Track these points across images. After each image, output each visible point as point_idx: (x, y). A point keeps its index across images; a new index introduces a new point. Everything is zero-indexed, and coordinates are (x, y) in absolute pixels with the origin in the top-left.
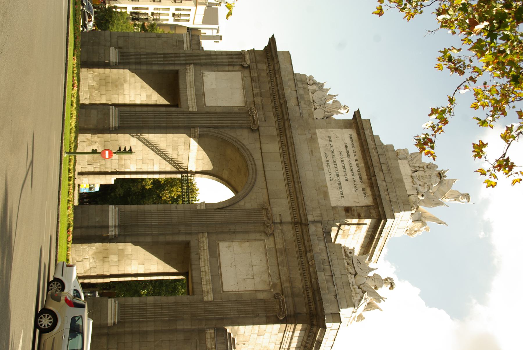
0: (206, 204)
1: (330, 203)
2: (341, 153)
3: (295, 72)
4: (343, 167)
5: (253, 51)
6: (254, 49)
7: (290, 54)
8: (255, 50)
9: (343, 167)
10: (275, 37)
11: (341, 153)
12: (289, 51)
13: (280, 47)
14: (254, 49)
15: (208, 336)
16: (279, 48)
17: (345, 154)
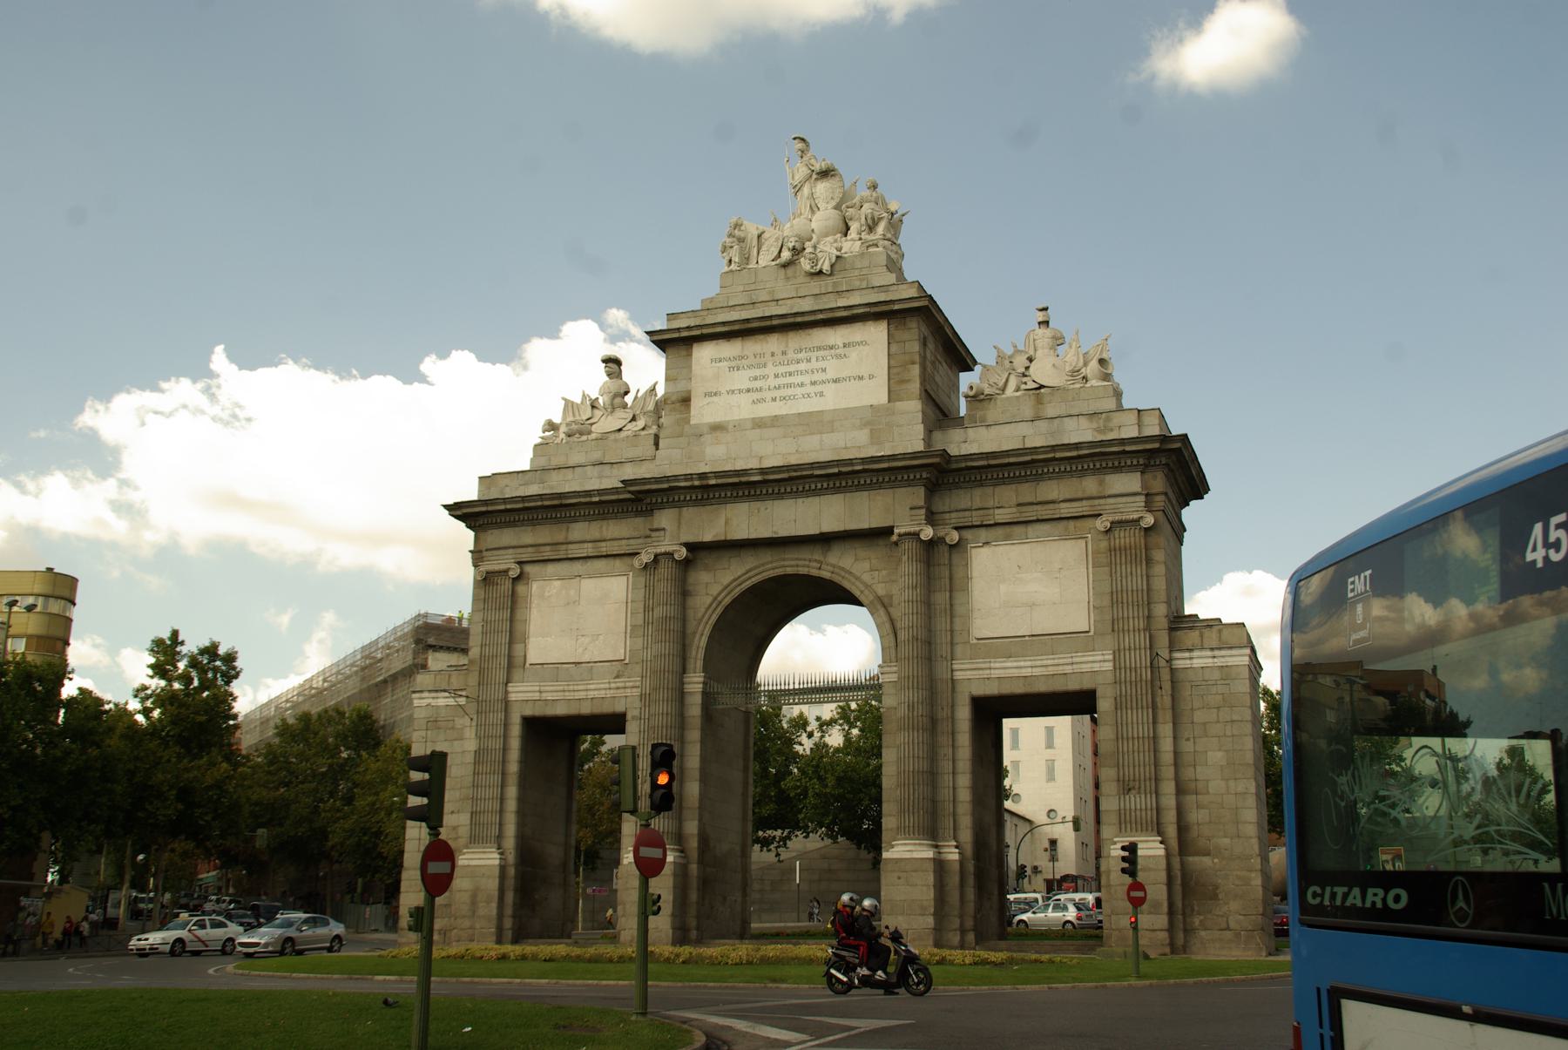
0: (884, 661)
1: (883, 405)
2: (756, 379)
3: (527, 467)
4: (790, 375)
5: (478, 555)
6: (470, 551)
7: (489, 474)
8: (472, 548)
9: (790, 375)
10: (451, 502)
11: (756, 379)
12: (480, 478)
13: (470, 493)
14: (470, 551)
15: (1187, 663)
16: (472, 494)
17: (757, 372)
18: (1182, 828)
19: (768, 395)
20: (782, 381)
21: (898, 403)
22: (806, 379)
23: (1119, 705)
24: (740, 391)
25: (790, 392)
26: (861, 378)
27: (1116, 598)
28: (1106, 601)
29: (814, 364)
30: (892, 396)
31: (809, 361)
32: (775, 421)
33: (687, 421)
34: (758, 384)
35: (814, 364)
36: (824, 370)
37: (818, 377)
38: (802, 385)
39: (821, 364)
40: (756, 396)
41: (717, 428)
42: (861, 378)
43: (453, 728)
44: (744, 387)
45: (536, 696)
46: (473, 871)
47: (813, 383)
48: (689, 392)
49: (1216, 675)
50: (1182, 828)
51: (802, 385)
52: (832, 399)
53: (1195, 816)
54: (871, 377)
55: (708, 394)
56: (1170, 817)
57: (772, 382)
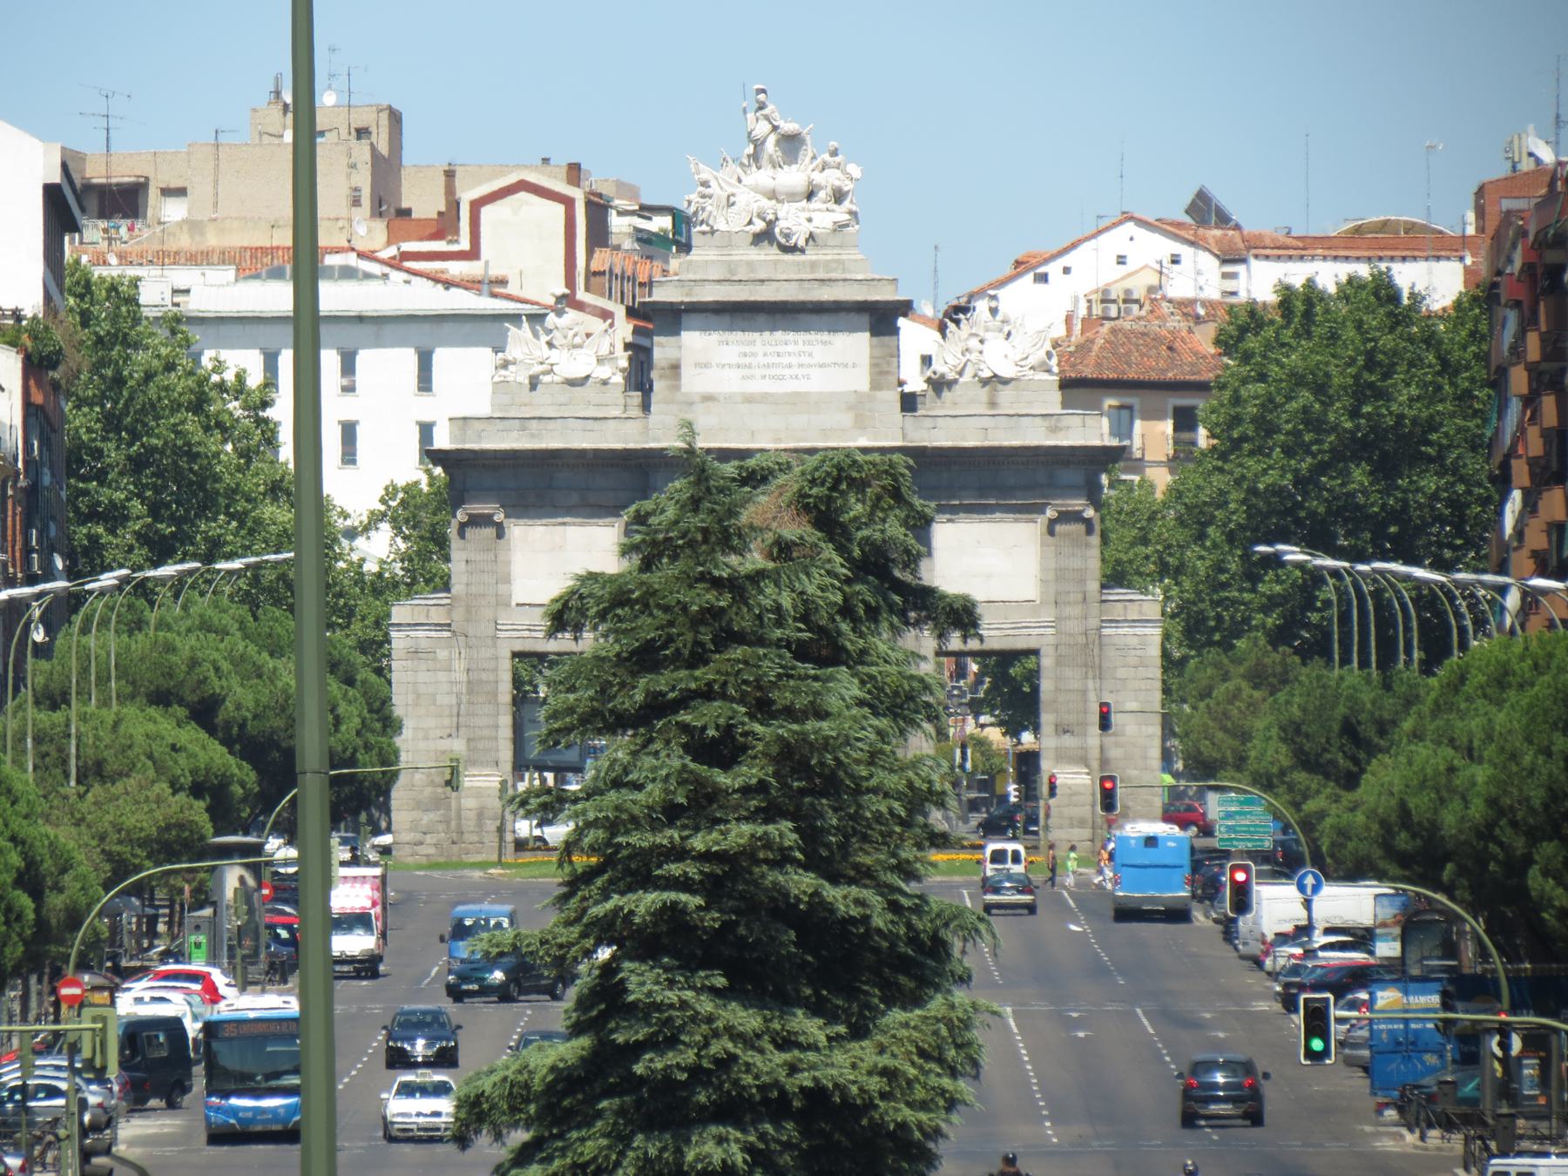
17: (747, 349)
18: (1104, 762)
19: (758, 372)
20: (770, 360)
21: (879, 394)
22: (794, 360)
23: (1059, 661)
24: (730, 366)
25: (779, 371)
26: (846, 366)
27: (1060, 575)
28: (1051, 576)
29: (801, 347)
30: (876, 385)
31: (796, 343)
32: (765, 398)
33: (677, 388)
34: (747, 360)
35: (801, 347)
36: (810, 355)
37: (805, 360)
38: (790, 366)
39: (807, 348)
40: (746, 372)
41: (708, 398)
42: (846, 366)
43: (434, 659)
44: (734, 361)
45: (526, 634)
46: (478, 793)
47: (801, 366)
48: (679, 360)
49: (1134, 642)
50: (1104, 762)
51: (790, 366)
52: (817, 382)
53: (1114, 753)
54: (854, 366)
55: (697, 365)
56: (1094, 754)
57: (761, 360)
